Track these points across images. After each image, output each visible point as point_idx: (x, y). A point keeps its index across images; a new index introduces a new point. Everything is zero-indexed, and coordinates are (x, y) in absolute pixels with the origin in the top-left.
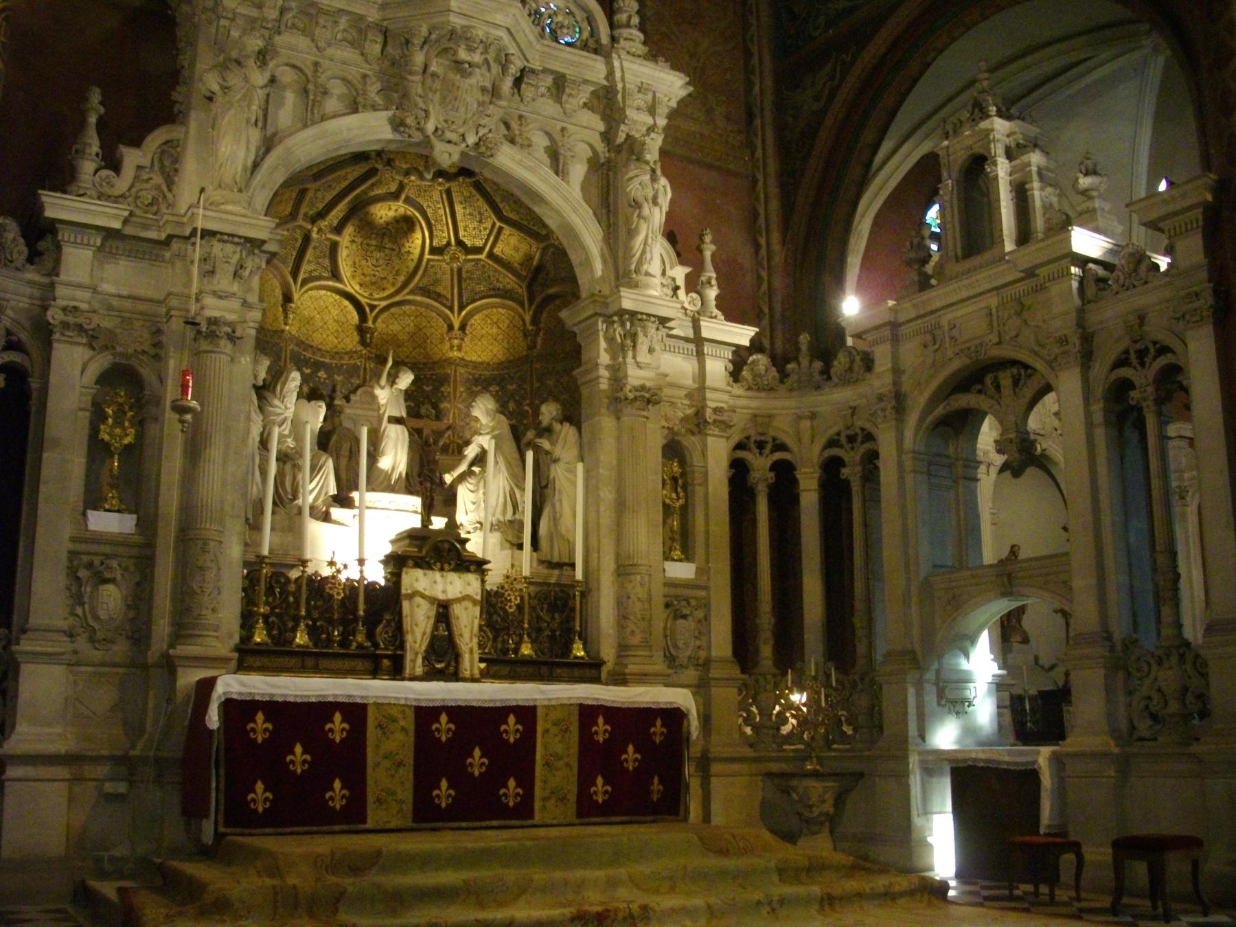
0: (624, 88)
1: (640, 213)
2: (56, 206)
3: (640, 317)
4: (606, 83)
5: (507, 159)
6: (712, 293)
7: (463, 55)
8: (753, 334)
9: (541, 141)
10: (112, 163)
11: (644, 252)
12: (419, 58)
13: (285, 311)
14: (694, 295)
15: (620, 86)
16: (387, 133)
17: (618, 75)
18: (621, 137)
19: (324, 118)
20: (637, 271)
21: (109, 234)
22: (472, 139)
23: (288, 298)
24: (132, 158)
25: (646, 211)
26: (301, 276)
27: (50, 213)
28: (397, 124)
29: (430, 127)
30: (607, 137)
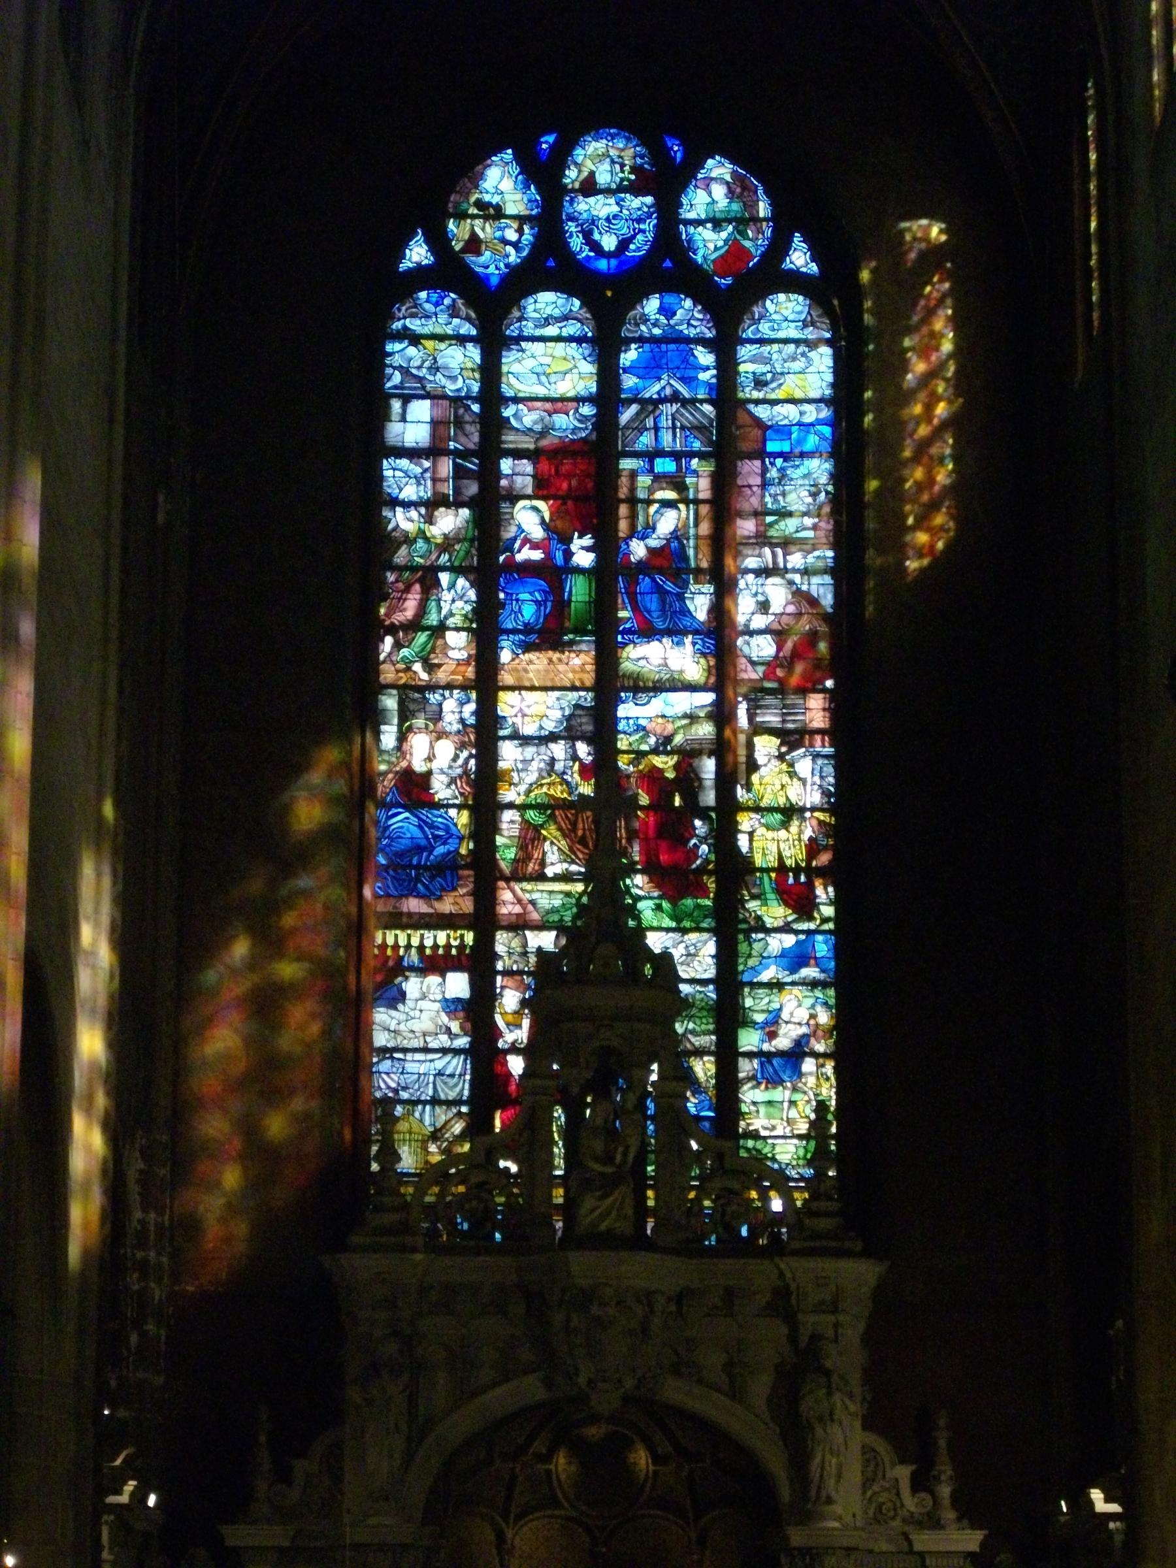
0: (798, 1288)
1: (813, 1435)
2: (236, 1535)
3: (814, 1551)
4: (779, 1283)
5: (675, 1392)
6: (945, 1491)
7: (595, 1310)
8: (982, 1537)
9: (712, 1360)
10: (284, 1476)
11: (821, 1476)
12: (558, 1318)
13: (499, 1553)
14: (923, 1495)
15: (793, 1286)
16: (541, 1394)
17: (788, 1275)
18: (804, 1341)
19: (474, 1395)
20: (818, 1497)
21: (281, 1550)
22: (629, 1383)
23: (500, 1537)
24: (301, 1467)
25: (819, 1431)
26: (514, 1510)
27: (230, 1542)
28: (548, 1383)
29: (582, 1380)
30: (793, 1339)
